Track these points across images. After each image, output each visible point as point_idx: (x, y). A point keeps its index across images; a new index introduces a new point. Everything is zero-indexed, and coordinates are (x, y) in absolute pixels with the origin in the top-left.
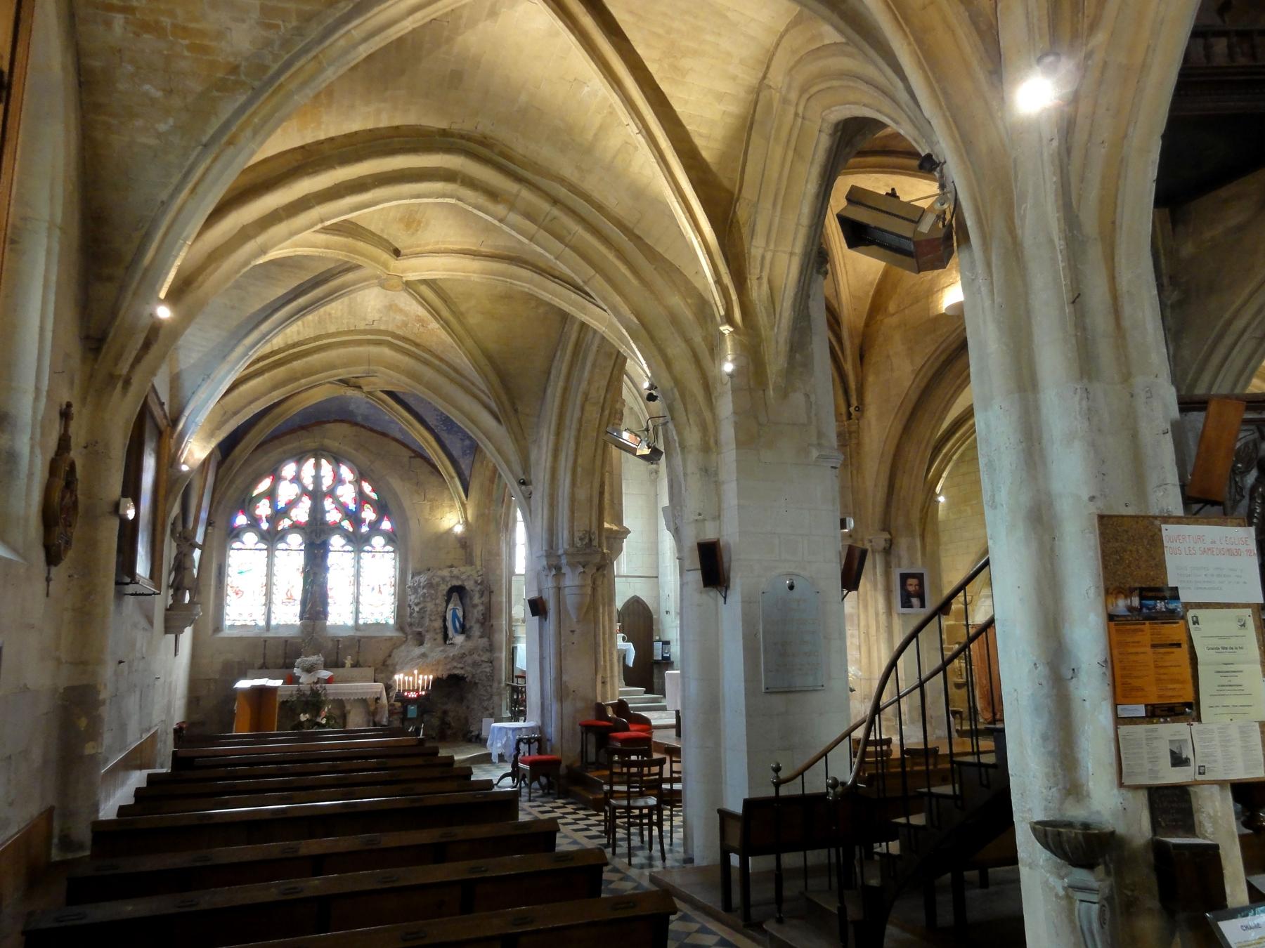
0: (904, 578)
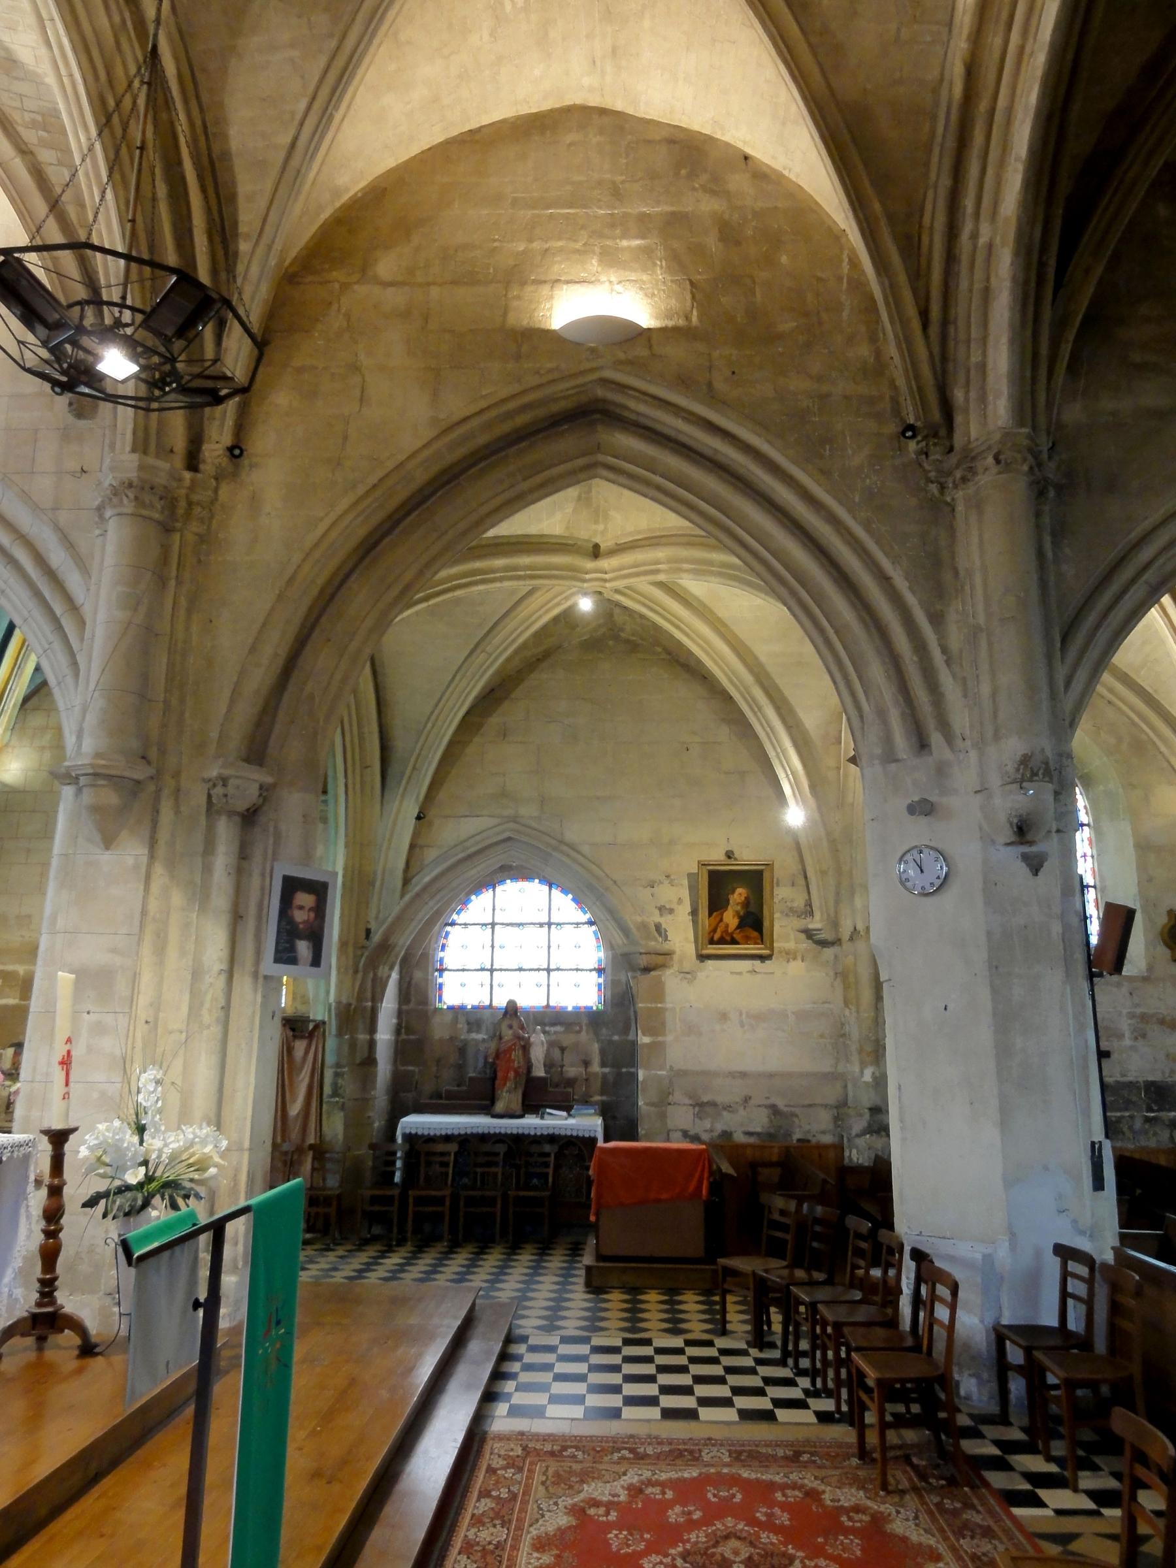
0: (291, 886)
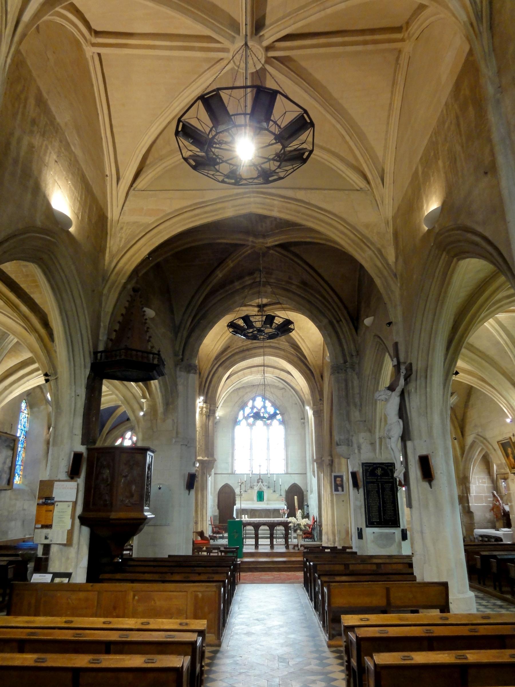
0: (336, 477)
